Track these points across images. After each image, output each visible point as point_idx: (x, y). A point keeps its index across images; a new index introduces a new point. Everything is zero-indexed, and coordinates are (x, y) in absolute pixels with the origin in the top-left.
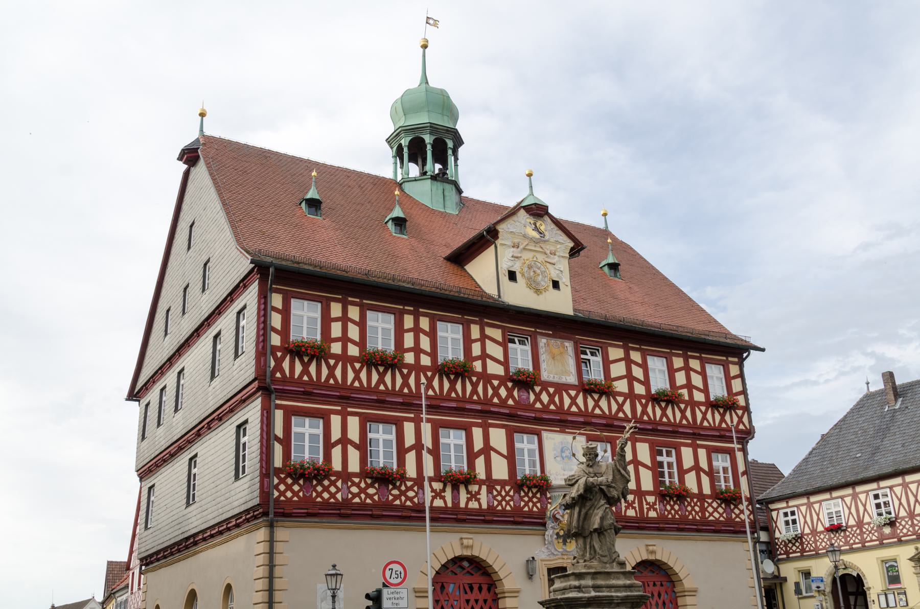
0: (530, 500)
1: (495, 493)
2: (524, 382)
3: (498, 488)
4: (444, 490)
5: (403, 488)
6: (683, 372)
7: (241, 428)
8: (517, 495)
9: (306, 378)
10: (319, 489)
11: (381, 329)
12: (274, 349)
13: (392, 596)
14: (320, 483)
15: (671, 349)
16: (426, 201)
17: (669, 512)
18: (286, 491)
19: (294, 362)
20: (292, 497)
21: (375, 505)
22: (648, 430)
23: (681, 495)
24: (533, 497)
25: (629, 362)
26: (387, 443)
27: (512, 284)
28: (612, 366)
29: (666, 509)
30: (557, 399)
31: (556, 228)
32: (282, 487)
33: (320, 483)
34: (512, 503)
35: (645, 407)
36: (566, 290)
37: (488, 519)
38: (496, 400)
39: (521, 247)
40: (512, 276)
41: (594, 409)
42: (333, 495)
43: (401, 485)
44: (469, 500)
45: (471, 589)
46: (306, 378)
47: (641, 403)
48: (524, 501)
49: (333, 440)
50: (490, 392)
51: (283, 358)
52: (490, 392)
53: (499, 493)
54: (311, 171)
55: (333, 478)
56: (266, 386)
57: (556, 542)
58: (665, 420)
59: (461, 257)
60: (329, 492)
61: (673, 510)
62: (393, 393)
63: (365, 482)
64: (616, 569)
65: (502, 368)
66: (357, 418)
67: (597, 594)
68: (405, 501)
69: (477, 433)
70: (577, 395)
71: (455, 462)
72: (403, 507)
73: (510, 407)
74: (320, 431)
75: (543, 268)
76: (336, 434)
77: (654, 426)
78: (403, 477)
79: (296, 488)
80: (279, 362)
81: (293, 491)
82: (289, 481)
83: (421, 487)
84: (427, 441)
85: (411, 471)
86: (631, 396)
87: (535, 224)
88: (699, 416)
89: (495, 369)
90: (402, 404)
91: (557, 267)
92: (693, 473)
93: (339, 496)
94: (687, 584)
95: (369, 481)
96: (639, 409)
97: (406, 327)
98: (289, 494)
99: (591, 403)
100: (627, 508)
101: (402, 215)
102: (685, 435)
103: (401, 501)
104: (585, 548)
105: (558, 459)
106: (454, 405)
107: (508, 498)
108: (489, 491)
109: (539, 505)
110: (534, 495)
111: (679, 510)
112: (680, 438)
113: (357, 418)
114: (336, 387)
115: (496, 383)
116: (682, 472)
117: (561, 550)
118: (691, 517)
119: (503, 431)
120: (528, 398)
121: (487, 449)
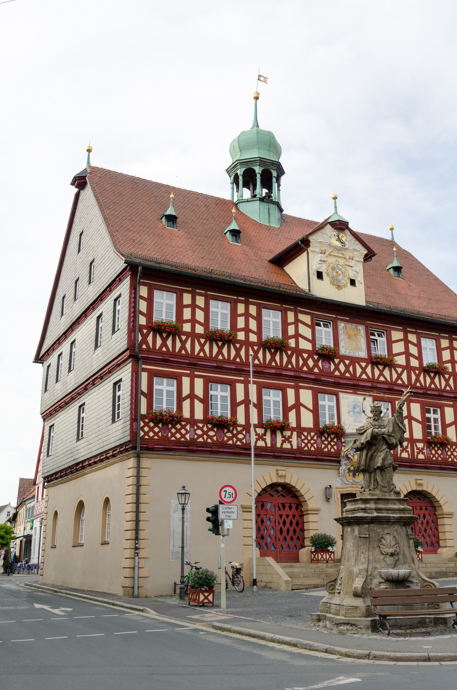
0: (329, 443)
1: (303, 437)
2: (327, 355)
3: (306, 434)
4: (265, 434)
5: (235, 432)
6: (448, 351)
7: (117, 384)
8: (319, 439)
9: (164, 349)
10: (173, 431)
11: (220, 314)
12: (141, 327)
13: (226, 510)
14: (174, 426)
15: (440, 333)
16: (255, 217)
17: (434, 456)
18: (149, 432)
20: (154, 436)
21: (214, 444)
22: (421, 394)
23: (443, 443)
24: (331, 441)
25: (407, 342)
26: (223, 398)
27: (320, 281)
28: (394, 345)
29: (431, 453)
30: (351, 369)
31: (354, 239)
32: (146, 429)
33: (174, 426)
34: (315, 445)
35: (418, 376)
36: (360, 287)
37: (297, 456)
38: (305, 369)
39: (327, 253)
40: (320, 275)
41: (379, 377)
42: (183, 436)
43: (233, 430)
44: (283, 442)
45: (284, 507)
46: (164, 349)
48: (324, 444)
49: (184, 395)
50: (301, 362)
51: (148, 334)
52: (301, 362)
53: (306, 438)
54: (170, 194)
55: (183, 423)
56: (135, 354)
57: (348, 475)
58: (433, 386)
59: (282, 260)
60: (181, 434)
61: (437, 454)
62: (228, 361)
63: (207, 427)
64: (393, 497)
65: (311, 344)
66: (201, 380)
67: (379, 515)
68: (236, 442)
69: (291, 393)
70: (366, 367)
71: (273, 414)
72: (234, 446)
73: (315, 374)
74: (174, 389)
75: (343, 270)
76: (186, 391)
77: (425, 391)
78: (235, 424)
79: (156, 430)
80: (145, 337)
81: (154, 432)
82: (152, 424)
83: (248, 432)
84: (253, 398)
85: (241, 420)
86: (408, 367)
87: (338, 236)
89: (305, 345)
90: (235, 370)
94: (446, 509)
95: (210, 426)
96: (414, 378)
98: (151, 434)
99: (377, 372)
100: (402, 451)
101: (237, 228)
102: (448, 399)
103: (233, 441)
104: (370, 481)
105: (351, 413)
106: (273, 371)
107: (312, 442)
108: (299, 436)
109: (335, 447)
110: (332, 440)
111: (442, 454)
112: (444, 400)
113: (201, 380)
114: (187, 356)
115: (305, 356)
116: (445, 426)
117: (351, 481)
118: (450, 460)
119: (310, 392)
120: (330, 367)
121: (298, 405)
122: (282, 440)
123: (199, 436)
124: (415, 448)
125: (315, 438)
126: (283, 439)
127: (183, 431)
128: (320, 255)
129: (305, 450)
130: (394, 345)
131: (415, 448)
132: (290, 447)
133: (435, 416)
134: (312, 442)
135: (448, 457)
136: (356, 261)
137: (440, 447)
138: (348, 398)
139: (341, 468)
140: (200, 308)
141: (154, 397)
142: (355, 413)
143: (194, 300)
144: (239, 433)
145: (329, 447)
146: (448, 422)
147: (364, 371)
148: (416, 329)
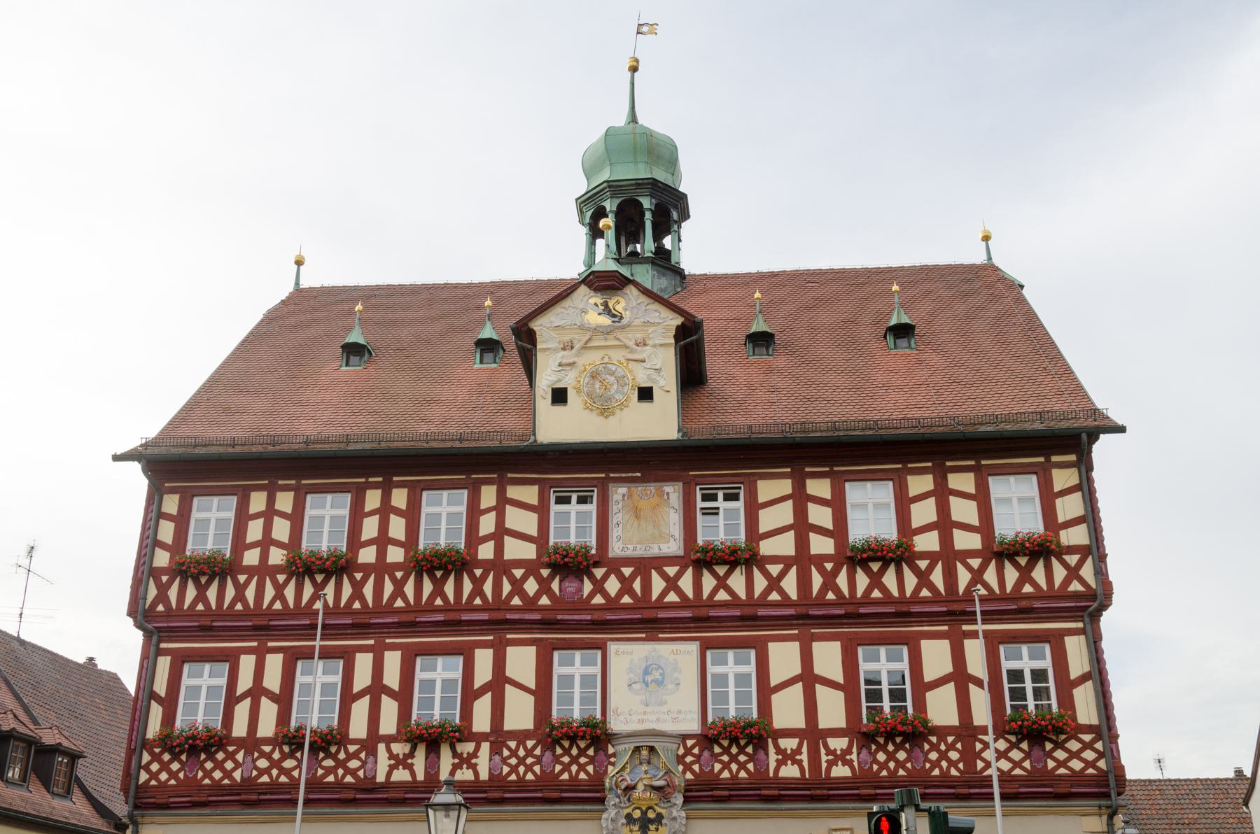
0: (574, 760)
1: (506, 753)
2: (570, 564)
3: (513, 744)
4: (411, 754)
5: (342, 756)
8: (548, 754)
10: (209, 765)
11: (326, 520)
14: (211, 757)
15: (904, 463)
18: (159, 772)
19: (186, 587)
23: (914, 733)
24: (579, 755)
26: (741, 679)
27: (559, 409)
28: (762, 513)
29: (875, 761)
30: (637, 586)
33: (211, 757)
34: (537, 769)
39: (577, 346)
40: (559, 396)
43: (338, 751)
44: (455, 767)
47: (822, 571)
48: (562, 763)
50: (507, 588)
51: (170, 583)
52: (507, 588)
55: (231, 749)
60: (223, 770)
63: (281, 751)
70: (679, 575)
72: (339, 785)
73: (544, 609)
75: (620, 372)
76: (245, 682)
77: (851, 609)
79: (175, 766)
81: (170, 772)
82: (166, 757)
83: (373, 752)
85: (358, 728)
87: (606, 305)
88: (964, 577)
89: (516, 550)
90: (353, 626)
93: (237, 775)
96: (817, 581)
100: (780, 763)
106: (439, 617)
109: (751, 766)
115: (518, 573)
116: (922, 688)
119: (532, 650)
120: (580, 590)
121: (499, 682)
122: (453, 764)
123: (261, 772)
124: (823, 751)
125: (538, 752)
126: (457, 761)
127: (229, 765)
128: (563, 353)
130: (1058, 501)
131: (823, 751)
133: (1038, 664)
134: (529, 760)
135: (928, 765)
136: (654, 346)
137: (903, 742)
138: (631, 653)
139: (605, 816)
140: (398, 512)
141: (338, 698)
142: (647, 685)
143: (271, 501)
144: (350, 756)
145: (573, 767)
146: (929, 676)
147: (672, 584)
148: (831, 466)
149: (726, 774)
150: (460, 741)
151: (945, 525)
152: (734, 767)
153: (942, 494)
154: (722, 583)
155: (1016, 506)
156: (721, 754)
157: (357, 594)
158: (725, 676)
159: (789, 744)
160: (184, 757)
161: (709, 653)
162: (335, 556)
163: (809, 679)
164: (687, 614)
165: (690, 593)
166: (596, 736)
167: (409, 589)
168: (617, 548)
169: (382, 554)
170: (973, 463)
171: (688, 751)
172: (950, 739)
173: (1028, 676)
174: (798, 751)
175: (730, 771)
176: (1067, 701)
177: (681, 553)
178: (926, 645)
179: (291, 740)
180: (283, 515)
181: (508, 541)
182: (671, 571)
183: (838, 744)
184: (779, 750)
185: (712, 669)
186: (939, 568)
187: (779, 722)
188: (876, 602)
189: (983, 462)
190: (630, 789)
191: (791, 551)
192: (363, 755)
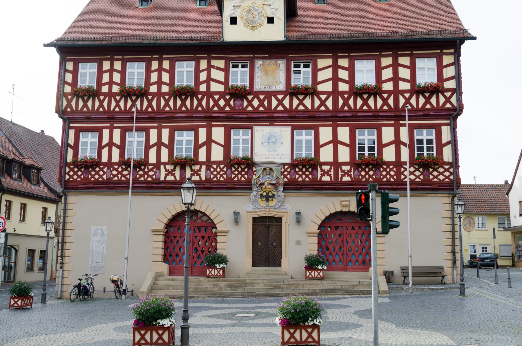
1: (212, 170)
2: (238, 94)
3: (215, 166)
4: (174, 170)
5: (146, 170)
9: (85, 109)
10: (93, 173)
11: (136, 73)
18: (73, 175)
20: (77, 178)
23: (377, 164)
24: (242, 171)
26: (308, 142)
27: (233, 26)
29: (361, 175)
30: (266, 103)
32: (71, 173)
33: (94, 170)
34: (225, 176)
38: (216, 109)
40: (233, 20)
42: (101, 176)
43: (145, 168)
47: (343, 98)
48: (235, 174)
49: (151, 144)
50: (212, 103)
51: (72, 99)
52: (212, 103)
55: (101, 167)
60: (99, 175)
63: (122, 168)
66: (119, 130)
70: (283, 99)
72: (146, 181)
73: (227, 112)
74: (312, 138)
76: (106, 140)
77: (354, 114)
79: (80, 173)
82: (76, 169)
84: (165, 139)
85: (152, 159)
88: (402, 101)
89: (215, 87)
91: (272, 7)
92: (393, 147)
93: (105, 177)
96: (341, 102)
97: (153, 69)
98: (75, 177)
100: (322, 175)
102: (388, 118)
103: (144, 178)
106: (184, 115)
108: (208, 169)
112: (383, 120)
113: (119, 130)
115: (216, 97)
116: (381, 146)
117: (264, 205)
119: (223, 129)
120: (242, 104)
121: (209, 142)
122: (191, 174)
123: (114, 176)
124: (340, 171)
125: (225, 169)
126: (192, 172)
127: (101, 173)
129: (214, 181)
131: (340, 171)
132: (199, 179)
133: (430, 137)
134: (222, 173)
135: (382, 177)
137: (372, 168)
139: (252, 194)
140: (166, 71)
143: (112, 65)
147: (280, 102)
149: (300, 179)
150: (194, 165)
151: (396, 79)
152: (304, 176)
153: (395, 66)
154: (301, 103)
155: (426, 71)
156: (299, 171)
157: (150, 105)
158: (301, 140)
159: (326, 168)
160: (83, 170)
161: (295, 131)
162: (140, 89)
163: (335, 142)
164: (287, 115)
165: (287, 106)
166: (248, 163)
167: (171, 103)
168: (257, 87)
169: (159, 88)
170: (410, 52)
171: (285, 170)
172: (391, 167)
173: (425, 142)
174: (330, 170)
175: (302, 178)
176: (440, 152)
177: (284, 89)
178: (384, 129)
179: (125, 163)
180: (117, 71)
181: (212, 83)
182: (280, 97)
183: (346, 168)
184: (322, 170)
185: (296, 138)
186: (392, 97)
187: (322, 159)
188: (365, 111)
189: (414, 52)
190: (262, 184)
191: (330, 89)
192: (155, 170)
